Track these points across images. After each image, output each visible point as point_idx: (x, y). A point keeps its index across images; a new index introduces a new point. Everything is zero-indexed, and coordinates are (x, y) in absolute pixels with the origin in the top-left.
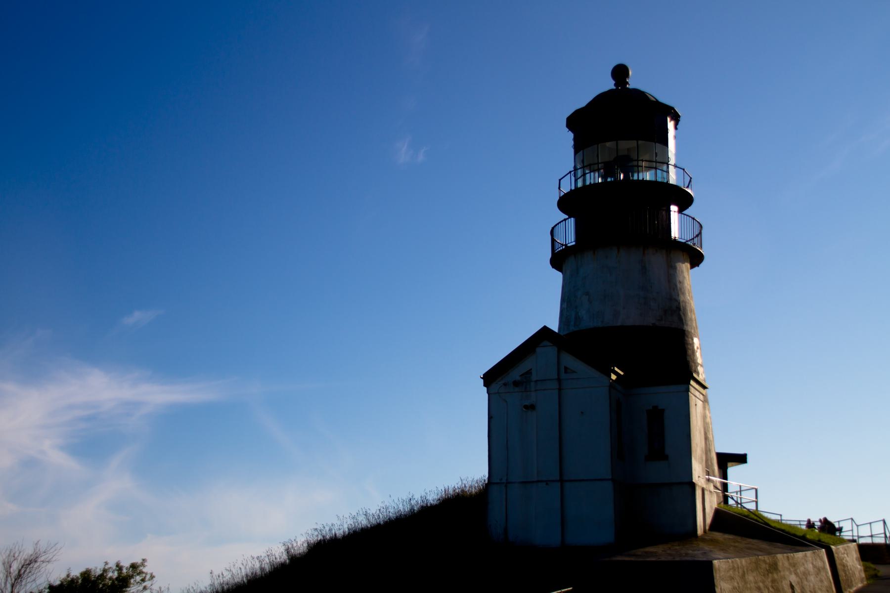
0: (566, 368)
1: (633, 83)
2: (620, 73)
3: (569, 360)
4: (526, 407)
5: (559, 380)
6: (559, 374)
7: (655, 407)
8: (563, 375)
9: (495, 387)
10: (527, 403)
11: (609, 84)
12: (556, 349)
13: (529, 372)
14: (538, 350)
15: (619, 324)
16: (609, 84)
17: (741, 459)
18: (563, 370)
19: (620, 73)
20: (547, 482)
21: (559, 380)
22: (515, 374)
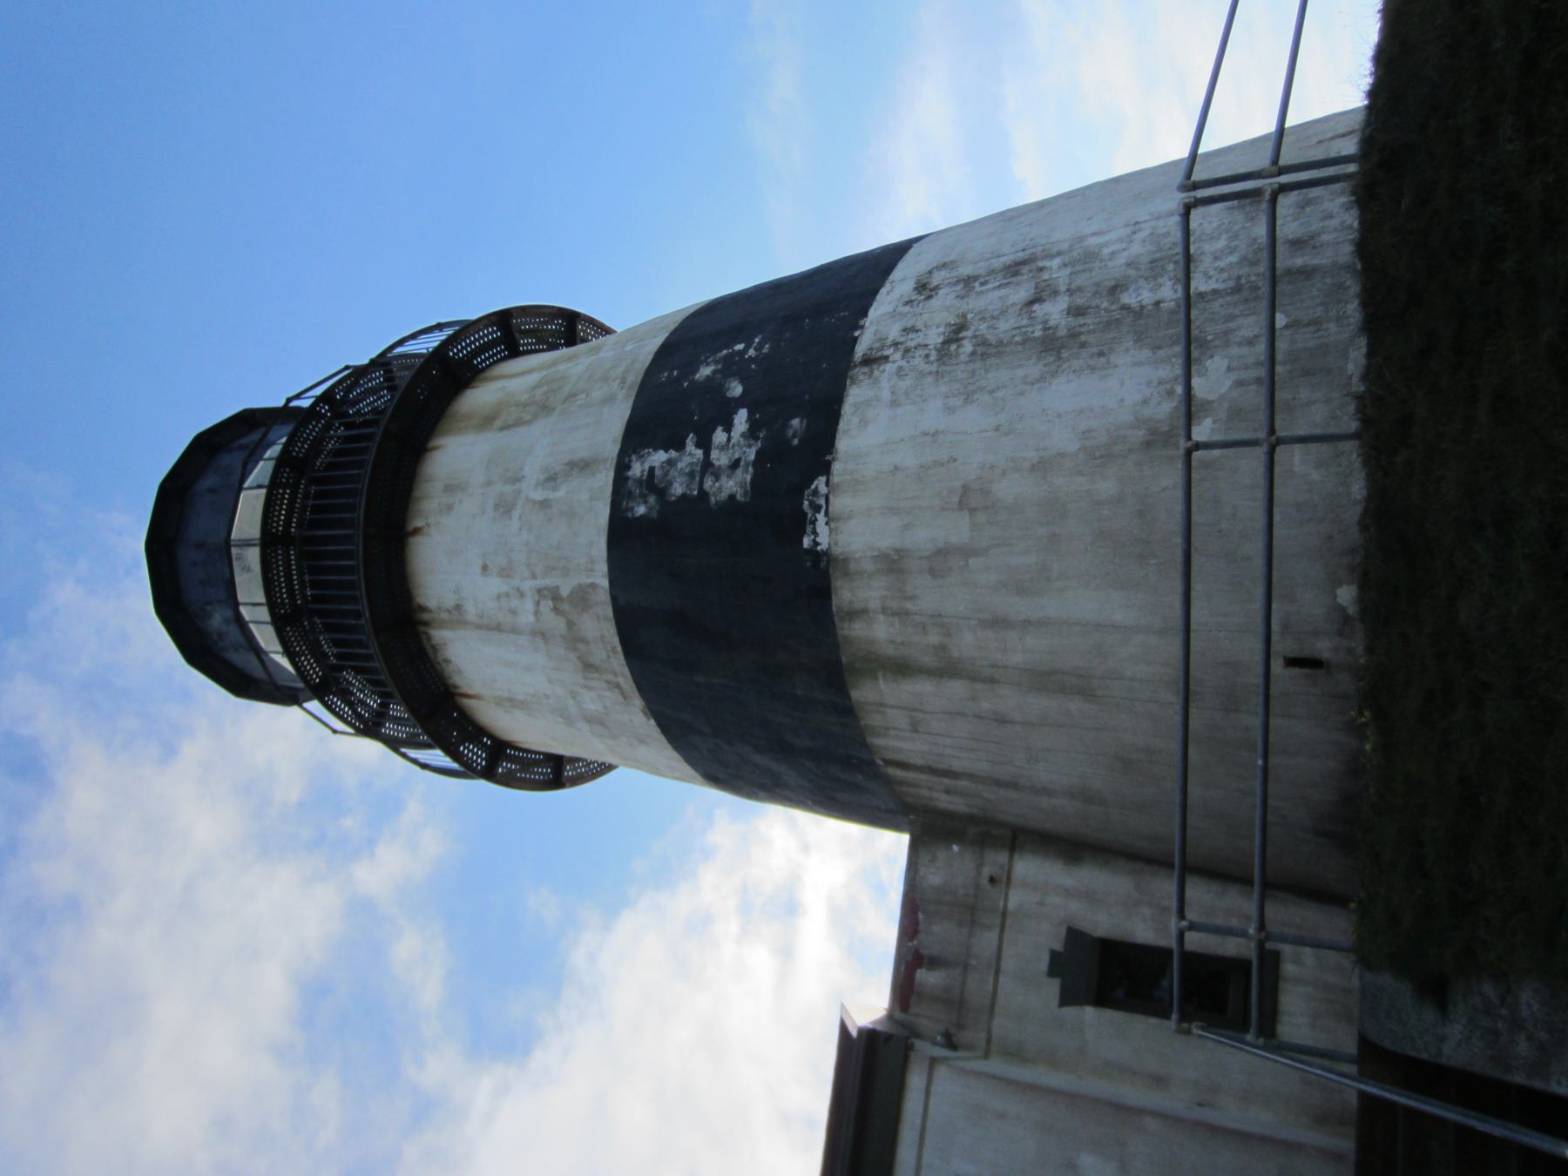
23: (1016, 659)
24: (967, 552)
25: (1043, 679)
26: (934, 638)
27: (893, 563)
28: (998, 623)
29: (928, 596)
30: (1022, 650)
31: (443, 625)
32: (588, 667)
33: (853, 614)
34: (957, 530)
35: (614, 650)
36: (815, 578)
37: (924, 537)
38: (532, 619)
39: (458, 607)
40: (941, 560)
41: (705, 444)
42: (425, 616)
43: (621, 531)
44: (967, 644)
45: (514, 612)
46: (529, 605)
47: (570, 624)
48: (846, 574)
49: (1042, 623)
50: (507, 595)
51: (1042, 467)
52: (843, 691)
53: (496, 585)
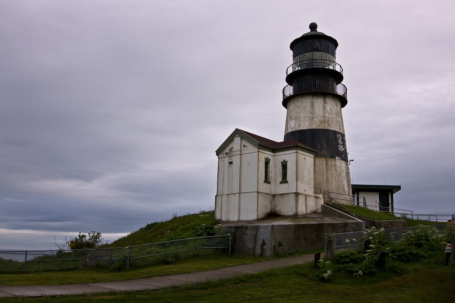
0: (244, 145)
1: (319, 30)
2: (313, 26)
3: (245, 143)
6: (241, 148)
7: (284, 160)
8: (243, 148)
10: (230, 161)
13: (232, 148)
15: (301, 129)
17: (398, 188)
18: (243, 146)
19: (313, 26)
21: (241, 151)
22: (227, 150)
23: (329, 176)
24: (337, 173)
25: (327, 178)
26: (330, 168)
27: (335, 166)
28: (332, 175)
29: (333, 169)
30: (330, 177)
31: (324, 100)
32: (321, 122)
33: (331, 160)
34: (338, 173)
35: (324, 128)
36: (333, 157)
37: (338, 169)
38: (326, 116)
39: (326, 103)
40: (336, 170)
41: (342, 145)
42: (325, 96)
43: (335, 132)
44: (330, 172)
45: (326, 113)
46: (328, 116)
47: (326, 122)
48: (334, 160)
49: (332, 179)
50: (328, 112)
51: (342, 181)
52: (323, 157)
53: (329, 111)
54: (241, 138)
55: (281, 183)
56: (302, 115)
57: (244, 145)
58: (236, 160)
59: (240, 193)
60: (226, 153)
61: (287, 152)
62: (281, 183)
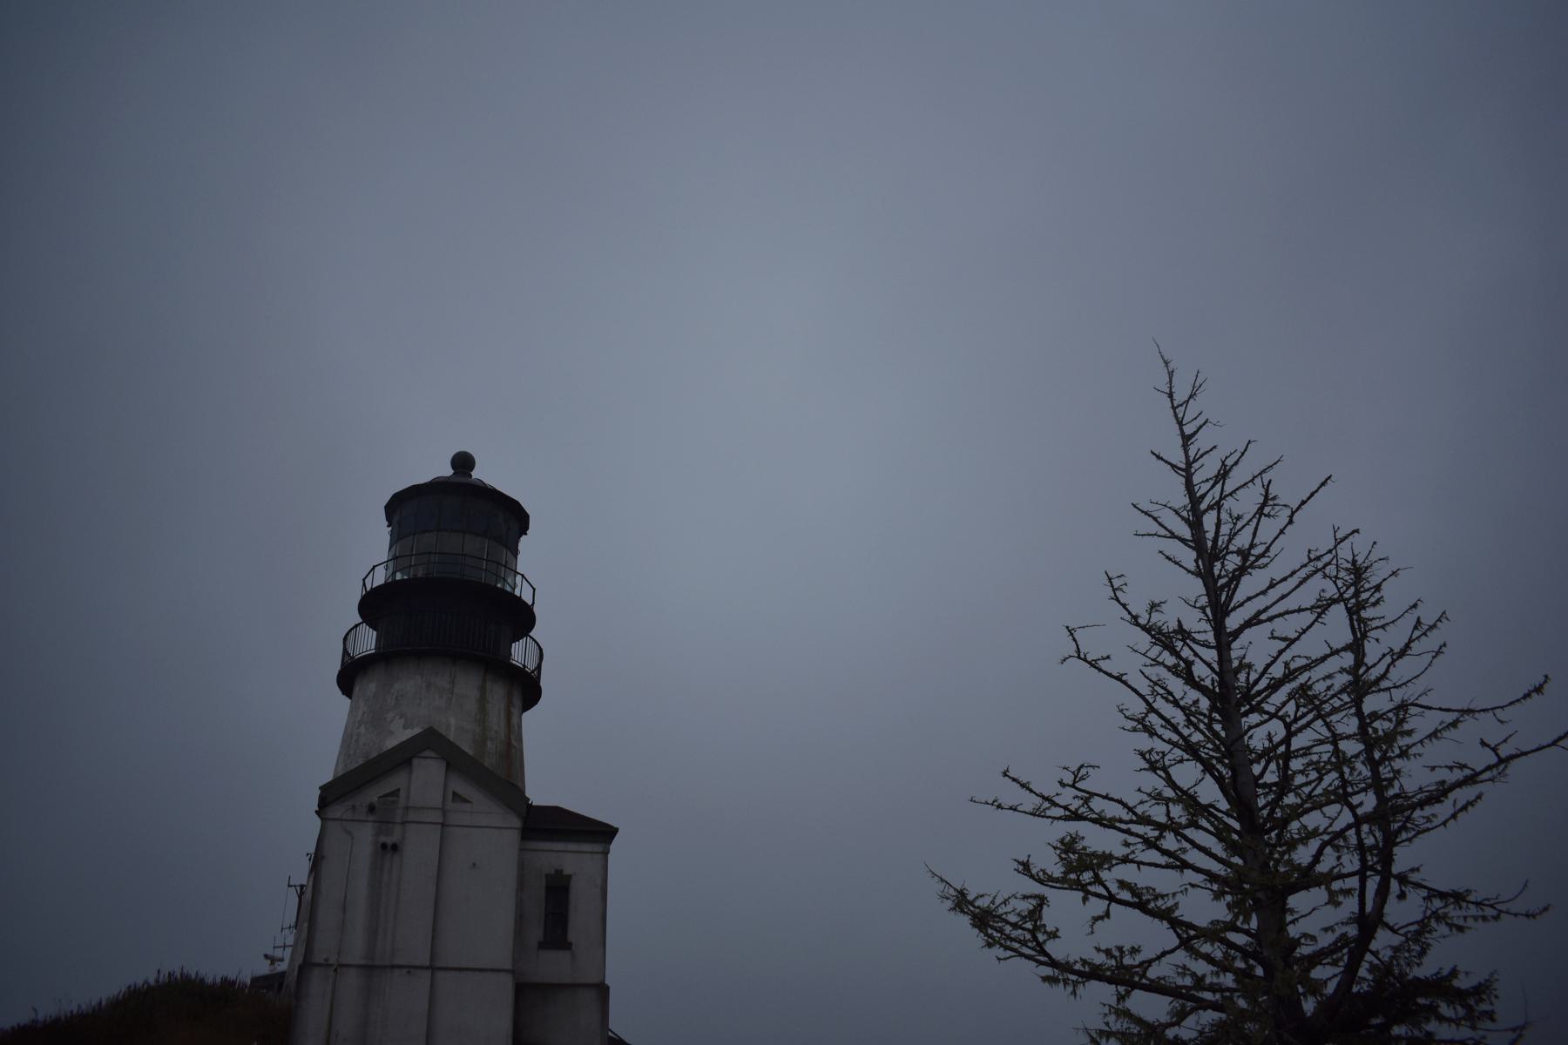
0: (454, 794)
2: (463, 462)
3: (460, 786)
4: (384, 846)
5: (444, 812)
7: (559, 872)
9: (337, 811)
10: (389, 841)
11: (448, 471)
12: (444, 765)
13: (396, 793)
14: (415, 762)
16: (448, 471)
18: (450, 796)
19: (463, 462)
20: (411, 968)
21: (444, 812)
22: (373, 795)
54: (449, 766)
55: (543, 946)
56: (453, 721)
57: (454, 794)
58: (420, 845)
59: (432, 968)
60: (372, 809)
61: (572, 846)
62: (543, 946)
